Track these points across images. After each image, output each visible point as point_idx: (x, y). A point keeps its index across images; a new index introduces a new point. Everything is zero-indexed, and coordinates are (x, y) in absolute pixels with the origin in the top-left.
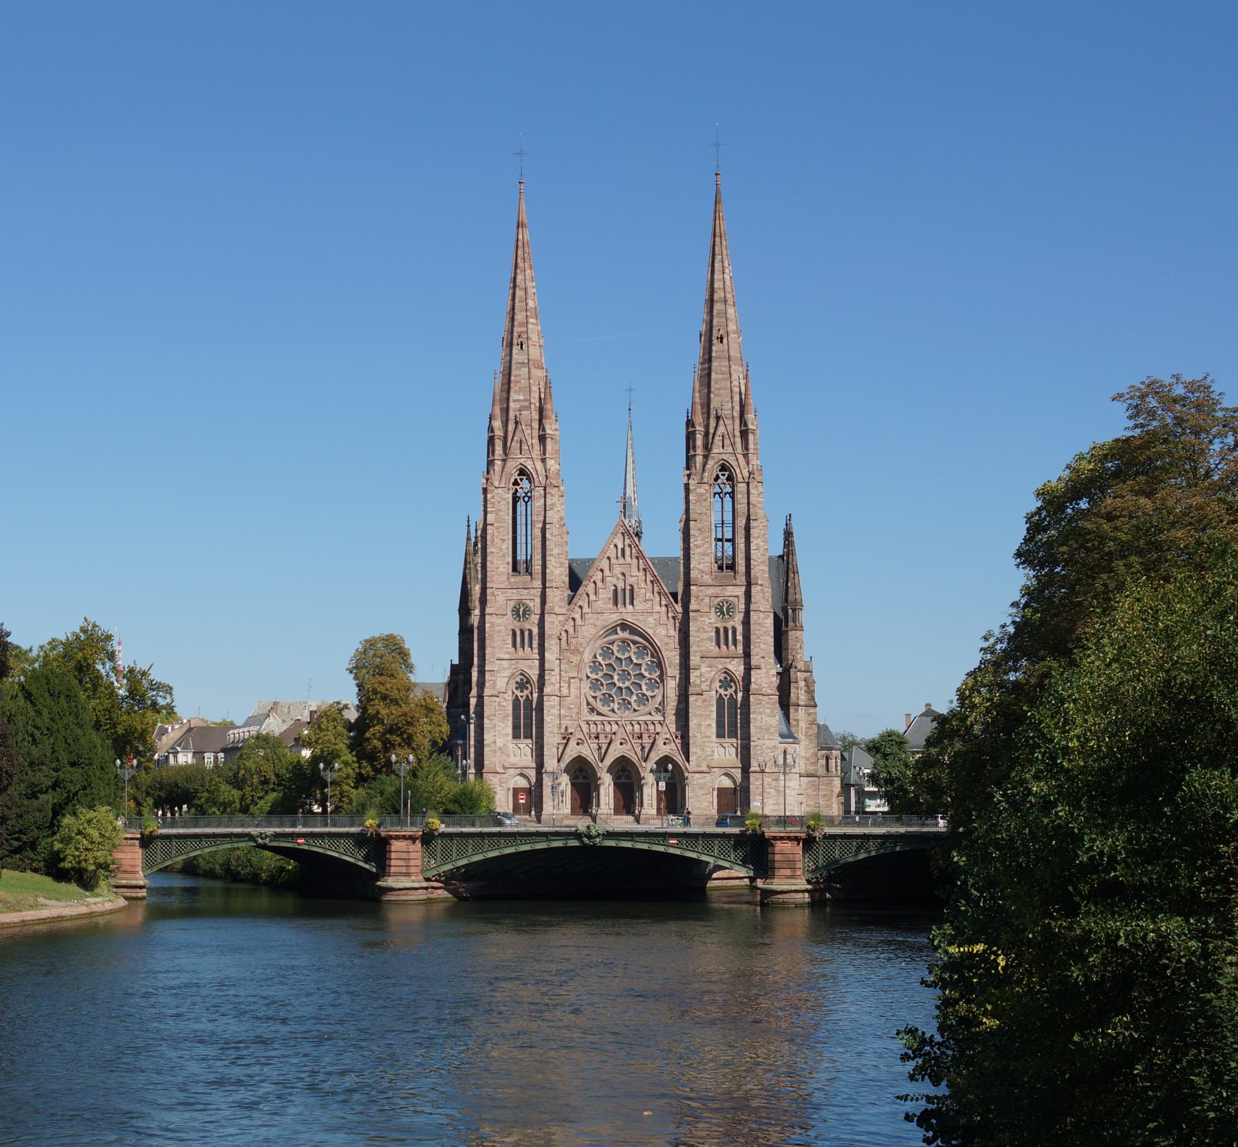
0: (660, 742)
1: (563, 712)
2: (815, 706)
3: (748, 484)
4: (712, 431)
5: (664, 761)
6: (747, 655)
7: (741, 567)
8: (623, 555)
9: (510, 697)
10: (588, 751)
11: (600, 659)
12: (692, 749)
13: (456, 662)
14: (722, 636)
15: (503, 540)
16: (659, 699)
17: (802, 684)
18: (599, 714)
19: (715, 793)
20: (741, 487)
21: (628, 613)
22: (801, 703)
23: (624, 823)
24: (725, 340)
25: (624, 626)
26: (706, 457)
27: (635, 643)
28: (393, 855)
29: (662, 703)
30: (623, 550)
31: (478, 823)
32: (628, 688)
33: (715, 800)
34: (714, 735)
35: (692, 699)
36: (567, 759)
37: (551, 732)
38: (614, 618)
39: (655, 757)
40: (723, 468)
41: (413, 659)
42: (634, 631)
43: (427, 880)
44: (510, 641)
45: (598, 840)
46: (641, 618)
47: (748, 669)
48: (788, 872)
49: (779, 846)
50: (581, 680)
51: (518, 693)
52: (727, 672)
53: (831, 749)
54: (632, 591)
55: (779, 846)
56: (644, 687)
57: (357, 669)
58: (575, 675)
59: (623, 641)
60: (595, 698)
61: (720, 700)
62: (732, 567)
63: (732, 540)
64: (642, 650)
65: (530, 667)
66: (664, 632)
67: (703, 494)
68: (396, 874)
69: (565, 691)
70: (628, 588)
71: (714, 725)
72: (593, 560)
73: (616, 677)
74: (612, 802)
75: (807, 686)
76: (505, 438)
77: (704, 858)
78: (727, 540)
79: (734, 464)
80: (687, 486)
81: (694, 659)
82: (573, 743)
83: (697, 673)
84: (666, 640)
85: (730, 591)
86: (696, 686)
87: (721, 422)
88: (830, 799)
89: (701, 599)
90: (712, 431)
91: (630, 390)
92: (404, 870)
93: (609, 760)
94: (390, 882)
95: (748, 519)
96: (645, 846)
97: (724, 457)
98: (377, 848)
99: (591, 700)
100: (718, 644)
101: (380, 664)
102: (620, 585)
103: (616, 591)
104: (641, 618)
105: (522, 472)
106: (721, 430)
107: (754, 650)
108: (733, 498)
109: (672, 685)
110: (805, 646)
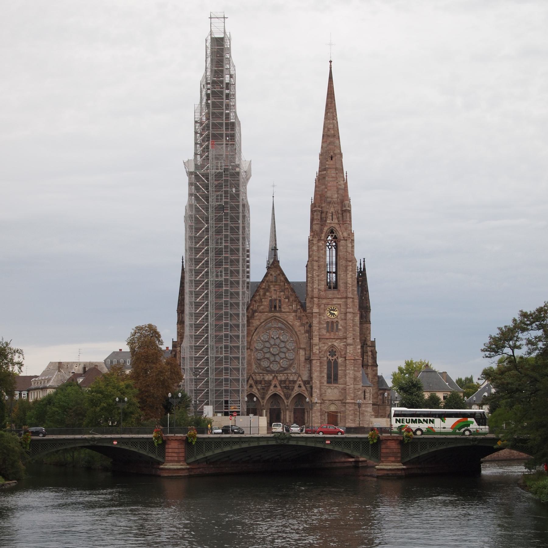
2: (377, 366)
13: (175, 340)
17: (370, 353)
19: (326, 414)
22: (370, 364)
24: (334, 159)
33: (326, 418)
39: (294, 394)
41: (162, 338)
43: (188, 464)
52: (333, 346)
62: (336, 287)
67: (321, 246)
68: (171, 461)
71: (326, 376)
78: (334, 273)
81: (316, 340)
83: (317, 347)
91: (274, 186)
92: (176, 459)
93: (267, 397)
96: (313, 445)
97: (333, 225)
100: (328, 331)
101: (145, 341)
108: (336, 249)
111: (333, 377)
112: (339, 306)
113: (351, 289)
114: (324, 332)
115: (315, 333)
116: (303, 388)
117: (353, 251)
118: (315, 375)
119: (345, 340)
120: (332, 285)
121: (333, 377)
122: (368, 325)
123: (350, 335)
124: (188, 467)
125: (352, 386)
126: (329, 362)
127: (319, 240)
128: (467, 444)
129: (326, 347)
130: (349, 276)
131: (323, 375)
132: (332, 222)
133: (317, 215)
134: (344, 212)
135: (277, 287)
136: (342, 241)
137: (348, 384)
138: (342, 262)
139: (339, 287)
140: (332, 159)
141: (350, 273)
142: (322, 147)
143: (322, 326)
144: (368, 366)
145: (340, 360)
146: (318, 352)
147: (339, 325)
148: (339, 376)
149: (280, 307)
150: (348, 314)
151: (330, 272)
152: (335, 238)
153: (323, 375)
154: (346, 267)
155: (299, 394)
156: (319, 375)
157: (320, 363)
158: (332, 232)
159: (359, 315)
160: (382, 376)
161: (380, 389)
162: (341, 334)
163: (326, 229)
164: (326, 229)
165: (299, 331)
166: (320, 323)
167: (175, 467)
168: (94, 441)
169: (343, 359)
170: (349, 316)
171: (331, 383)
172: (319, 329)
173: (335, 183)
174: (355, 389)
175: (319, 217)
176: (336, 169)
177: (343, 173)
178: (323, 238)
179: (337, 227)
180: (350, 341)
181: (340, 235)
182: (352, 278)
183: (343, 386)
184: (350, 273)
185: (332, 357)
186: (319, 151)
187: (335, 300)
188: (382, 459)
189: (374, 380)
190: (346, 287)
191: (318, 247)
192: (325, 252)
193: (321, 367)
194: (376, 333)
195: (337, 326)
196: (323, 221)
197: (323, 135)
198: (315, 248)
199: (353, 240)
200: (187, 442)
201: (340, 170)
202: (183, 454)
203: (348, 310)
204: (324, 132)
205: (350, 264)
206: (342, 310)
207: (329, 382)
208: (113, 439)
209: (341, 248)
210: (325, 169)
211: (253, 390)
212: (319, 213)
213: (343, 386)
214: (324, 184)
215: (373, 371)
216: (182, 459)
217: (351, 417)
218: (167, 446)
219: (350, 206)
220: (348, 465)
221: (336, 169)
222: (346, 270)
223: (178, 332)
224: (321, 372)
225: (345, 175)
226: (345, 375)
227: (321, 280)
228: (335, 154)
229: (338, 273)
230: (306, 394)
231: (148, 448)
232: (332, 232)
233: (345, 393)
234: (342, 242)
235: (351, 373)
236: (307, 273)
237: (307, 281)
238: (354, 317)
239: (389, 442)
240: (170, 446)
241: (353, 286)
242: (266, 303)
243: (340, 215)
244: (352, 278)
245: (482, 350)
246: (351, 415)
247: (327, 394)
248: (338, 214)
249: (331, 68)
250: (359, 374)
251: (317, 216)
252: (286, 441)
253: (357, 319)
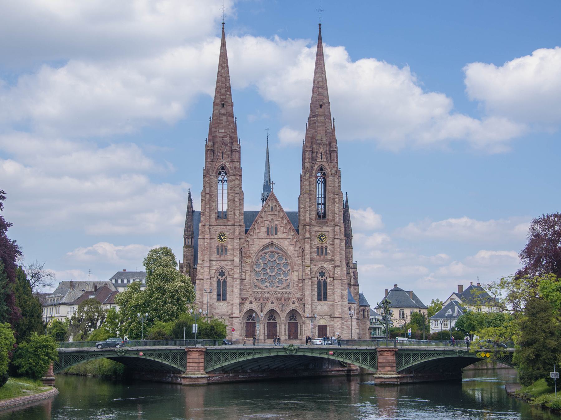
1: (242, 287)
2: (358, 285)
11: (261, 261)
15: (214, 202)
17: (352, 274)
18: (259, 288)
19: (317, 328)
21: (274, 239)
23: (270, 344)
24: (323, 107)
25: (272, 244)
27: (278, 253)
31: (217, 343)
33: (317, 331)
34: (316, 300)
37: (237, 297)
38: (268, 241)
39: (288, 310)
42: (277, 247)
43: (207, 373)
44: (216, 252)
46: (281, 241)
50: (251, 272)
51: (220, 277)
52: (322, 268)
54: (276, 228)
58: (248, 268)
59: (272, 252)
62: (325, 216)
63: (325, 204)
64: (280, 257)
65: (227, 265)
66: (292, 248)
67: (312, 181)
68: (192, 371)
69: (243, 277)
71: (316, 294)
72: (258, 212)
74: (266, 332)
75: (354, 275)
77: (347, 361)
79: (327, 167)
81: (308, 262)
83: (309, 269)
84: (293, 252)
85: (325, 229)
86: (308, 275)
88: (365, 331)
92: (196, 368)
99: (256, 281)
100: (318, 255)
104: (281, 241)
105: (223, 168)
111: (322, 295)
112: (327, 233)
113: (338, 219)
114: (315, 255)
115: (308, 256)
116: (297, 304)
117: (339, 186)
118: (307, 293)
119: (333, 263)
120: (322, 215)
121: (322, 295)
122: (350, 250)
123: (337, 258)
124: (207, 375)
125: (339, 303)
126: (319, 282)
127: (311, 176)
128: (454, 356)
129: (316, 269)
130: (336, 207)
131: (314, 293)
132: (321, 161)
133: (309, 155)
134: (331, 152)
136: (330, 177)
137: (337, 301)
138: (330, 195)
139: (327, 217)
140: (321, 107)
141: (337, 205)
142: (312, 97)
143: (313, 250)
144: (351, 285)
145: (329, 280)
146: (309, 273)
147: (328, 250)
148: (328, 294)
150: (335, 240)
151: (319, 204)
152: (324, 174)
153: (314, 293)
154: (334, 199)
155: (293, 310)
156: (310, 292)
157: (312, 282)
158: (321, 169)
159: (345, 241)
160: (362, 295)
161: (361, 306)
162: (329, 257)
163: (316, 166)
164: (316, 166)
166: (311, 247)
167: (196, 376)
168: (122, 353)
169: (332, 279)
170: (337, 242)
171: (321, 300)
172: (311, 253)
173: (324, 128)
174: (342, 306)
175: (310, 156)
176: (325, 116)
177: (331, 119)
178: (313, 174)
179: (326, 165)
180: (337, 263)
181: (328, 171)
182: (339, 209)
183: (331, 303)
184: (337, 205)
185: (322, 277)
186: (310, 100)
187: (324, 227)
188: (380, 369)
189: (356, 298)
190: (334, 217)
191: (310, 182)
192: (316, 186)
193: (312, 286)
194: (356, 257)
195: (326, 250)
196: (313, 160)
197: (314, 87)
198: (307, 183)
199: (340, 176)
200: (207, 354)
201: (328, 116)
202: (202, 364)
203: (336, 237)
204: (314, 84)
205: (337, 196)
206: (330, 236)
207: (319, 299)
208: (138, 351)
209: (330, 183)
210: (315, 116)
212: (311, 153)
213: (331, 303)
214: (314, 128)
215: (355, 290)
216: (202, 368)
217: (338, 330)
218: (188, 357)
219: (336, 147)
220: (341, 373)
221: (325, 116)
222: (334, 203)
223: (184, 255)
224: (312, 290)
225: (332, 121)
226: (334, 293)
227: (312, 211)
228: (324, 104)
229: (327, 204)
230: (300, 311)
231: (170, 358)
232: (321, 169)
233: (334, 309)
234: (331, 178)
235: (337, 292)
236: (299, 204)
237: (299, 211)
238: (341, 243)
239: (385, 353)
240: (191, 357)
241: (339, 215)
242: (264, 229)
243: (328, 155)
244: (339, 209)
246: (339, 329)
247: (318, 310)
248: (327, 154)
249: (320, 30)
250: (346, 293)
251: (308, 155)
252: (294, 352)
253: (344, 244)
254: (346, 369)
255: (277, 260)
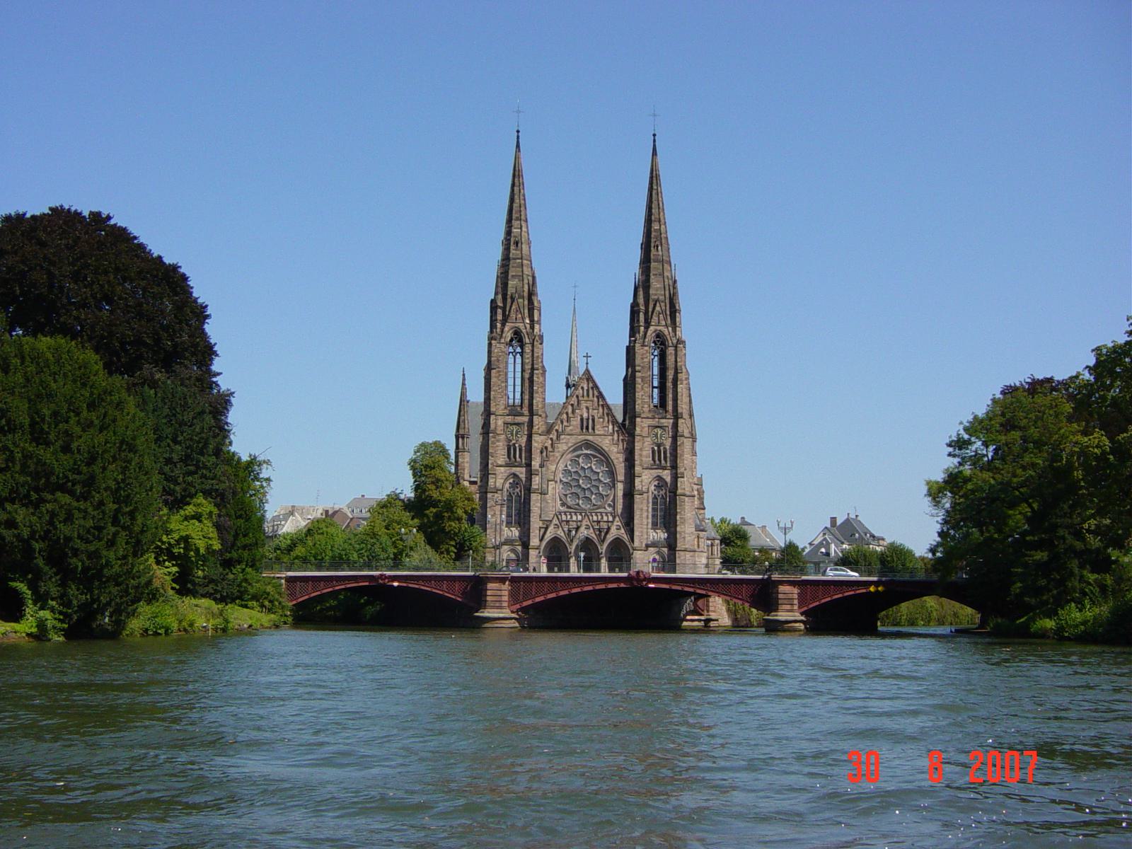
0: (613, 529)
2: (704, 509)
3: (676, 347)
4: (650, 310)
5: (617, 543)
6: (674, 467)
7: (670, 408)
8: (588, 395)
9: (505, 493)
10: (560, 533)
12: (636, 533)
14: (657, 453)
16: (612, 498)
20: (671, 351)
25: (588, 445)
26: (647, 328)
28: (489, 593)
29: (614, 501)
30: (588, 390)
32: (589, 488)
35: (637, 498)
36: (548, 536)
39: (610, 538)
40: (658, 336)
42: (596, 449)
45: (644, 583)
47: (675, 477)
48: (788, 607)
49: (782, 588)
50: (556, 482)
53: (714, 539)
54: (593, 420)
55: (782, 588)
56: (601, 489)
57: (413, 465)
59: (587, 455)
60: (566, 495)
61: (655, 498)
70: (591, 418)
73: (581, 481)
75: (699, 494)
76: (504, 309)
80: (630, 352)
81: (638, 469)
82: (551, 529)
87: (658, 304)
89: (642, 426)
90: (650, 310)
91: (575, 287)
94: (487, 613)
95: (676, 372)
98: (476, 589)
99: (563, 497)
102: (585, 415)
103: (582, 420)
106: (658, 308)
107: (680, 464)
109: (620, 487)
110: (697, 467)
135: (589, 404)
149: (593, 429)
155: (618, 538)
165: (617, 459)
211: (559, 533)
225: (673, 268)
242: (576, 422)
245: (949, 445)
254: (703, 618)
255: (594, 467)
